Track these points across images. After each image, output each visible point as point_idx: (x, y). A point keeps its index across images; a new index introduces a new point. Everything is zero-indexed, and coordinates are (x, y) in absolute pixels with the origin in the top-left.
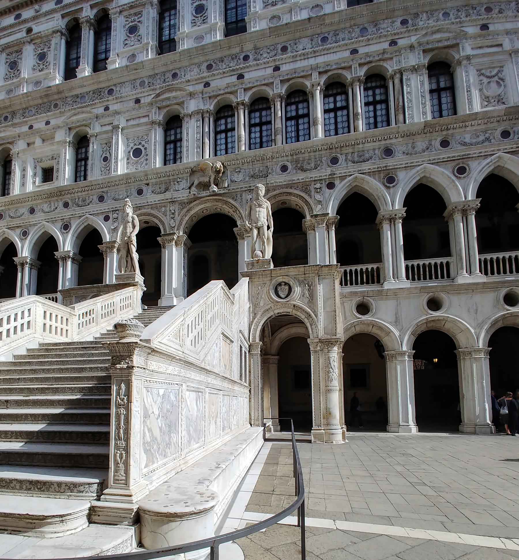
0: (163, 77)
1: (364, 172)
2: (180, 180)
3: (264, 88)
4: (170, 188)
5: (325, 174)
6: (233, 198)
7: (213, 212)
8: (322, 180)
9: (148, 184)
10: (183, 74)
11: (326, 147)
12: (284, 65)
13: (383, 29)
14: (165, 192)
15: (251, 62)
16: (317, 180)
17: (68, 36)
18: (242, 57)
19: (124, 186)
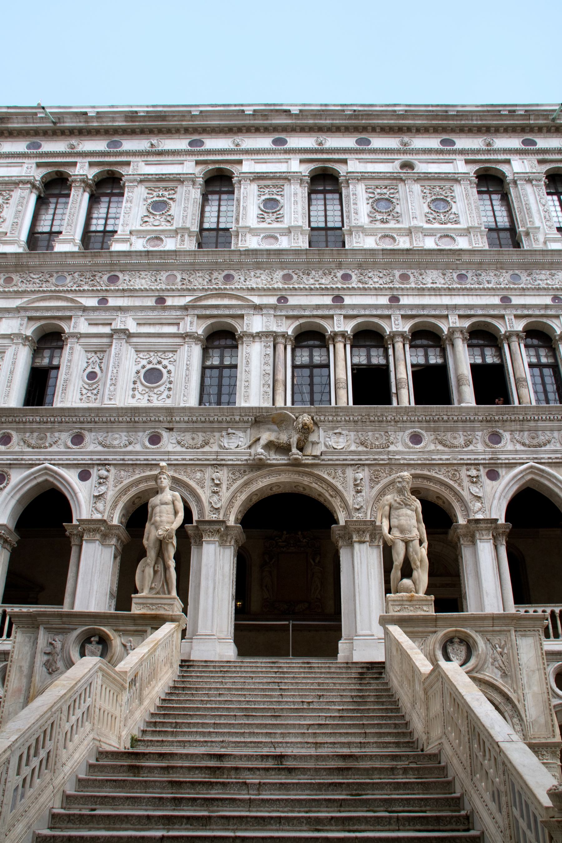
0: (207, 276)
1: (543, 461)
2: (234, 431)
3: (376, 320)
4: (212, 441)
5: (483, 457)
6: (329, 474)
7: (287, 490)
8: (478, 464)
9: (171, 429)
10: (243, 279)
11: (480, 418)
12: (405, 297)
13: (541, 280)
14: (202, 447)
15: (354, 283)
16: (471, 464)
17: (42, 190)
18: (340, 274)
19: (124, 425)
